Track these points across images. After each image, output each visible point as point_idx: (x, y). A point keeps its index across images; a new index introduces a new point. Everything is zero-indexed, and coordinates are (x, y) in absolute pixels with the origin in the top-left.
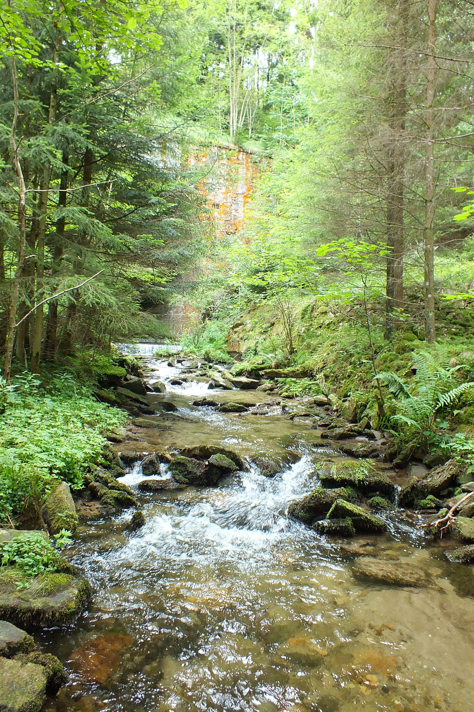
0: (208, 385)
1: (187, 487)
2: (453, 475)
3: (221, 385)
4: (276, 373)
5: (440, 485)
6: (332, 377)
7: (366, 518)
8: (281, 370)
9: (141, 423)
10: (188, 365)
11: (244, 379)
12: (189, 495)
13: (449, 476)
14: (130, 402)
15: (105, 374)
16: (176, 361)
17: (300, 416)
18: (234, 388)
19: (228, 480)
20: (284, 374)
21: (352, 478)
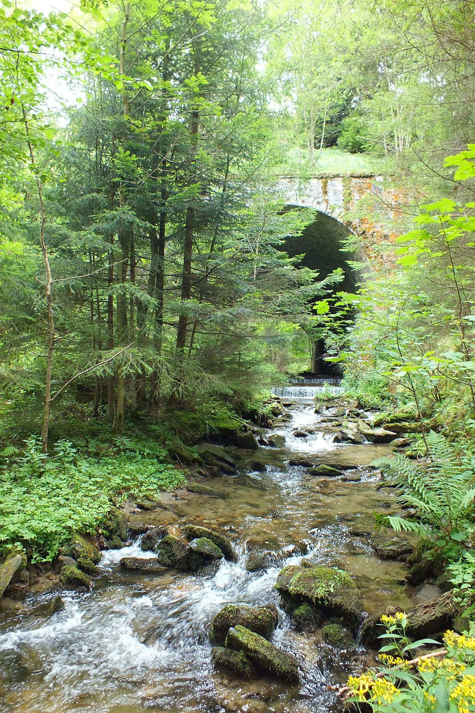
0: (333, 438)
1: (167, 570)
2: (445, 615)
3: (349, 439)
4: (401, 427)
5: (421, 626)
6: (452, 436)
7: (266, 657)
8: (407, 424)
9: (194, 487)
10: (334, 413)
11: (380, 431)
12: (168, 578)
13: (440, 615)
14: (215, 461)
15: (218, 428)
16: (324, 407)
17: (389, 486)
18: (366, 442)
19: (208, 569)
20: (410, 428)
21: (310, 594)
